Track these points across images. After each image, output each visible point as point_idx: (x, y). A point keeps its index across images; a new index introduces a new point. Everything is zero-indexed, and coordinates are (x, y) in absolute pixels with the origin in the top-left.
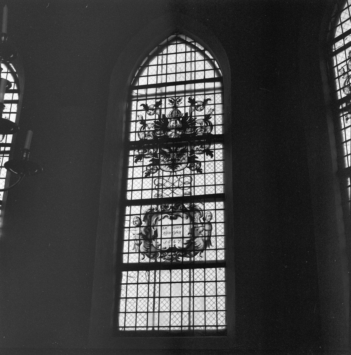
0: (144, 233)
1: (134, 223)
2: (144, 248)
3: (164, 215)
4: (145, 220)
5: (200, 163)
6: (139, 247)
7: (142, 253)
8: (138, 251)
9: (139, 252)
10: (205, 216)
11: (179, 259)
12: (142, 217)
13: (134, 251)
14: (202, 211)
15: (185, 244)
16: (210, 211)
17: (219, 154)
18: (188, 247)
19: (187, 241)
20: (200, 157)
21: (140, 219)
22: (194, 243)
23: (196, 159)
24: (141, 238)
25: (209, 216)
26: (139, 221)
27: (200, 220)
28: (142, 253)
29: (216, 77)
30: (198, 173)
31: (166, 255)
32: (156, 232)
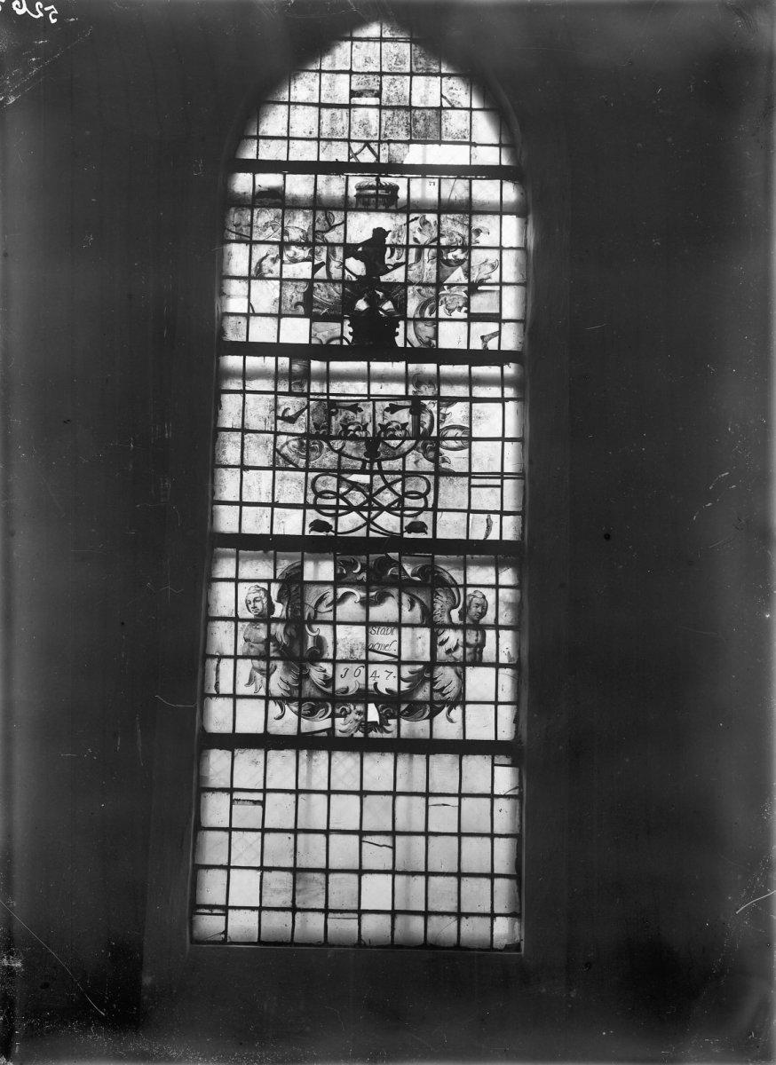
0: (281, 638)
1: (250, 606)
2: (283, 685)
3: (341, 591)
4: (282, 601)
6: (265, 680)
7: (275, 699)
8: (262, 692)
9: (268, 698)
10: (468, 602)
11: (389, 725)
12: (275, 588)
13: (250, 690)
14: (457, 586)
15: (405, 681)
16: (482, 590)
18: (414, 688)
19: (410, 672)
21: (268, 593)
22: (433, 681)
24: (274, 652)
25: (478, 605)
26: (265, 600)
27: (450, 618)
28: (275, 699)
29: (504, 163)
31: (351, 712)
32: (319, 641)
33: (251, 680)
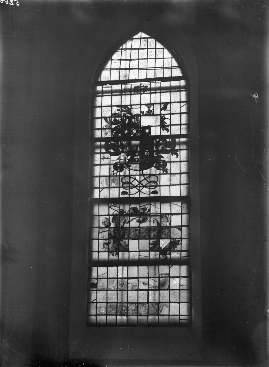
5: (165, 163)
12: (111, 217)
13: (104, 250)
15: (151, 244)
17: (183, 154)
20: (165, 157)
21: (109, 219)
23: (162, 159)
30: (163, 172)
33: (104, 247)
